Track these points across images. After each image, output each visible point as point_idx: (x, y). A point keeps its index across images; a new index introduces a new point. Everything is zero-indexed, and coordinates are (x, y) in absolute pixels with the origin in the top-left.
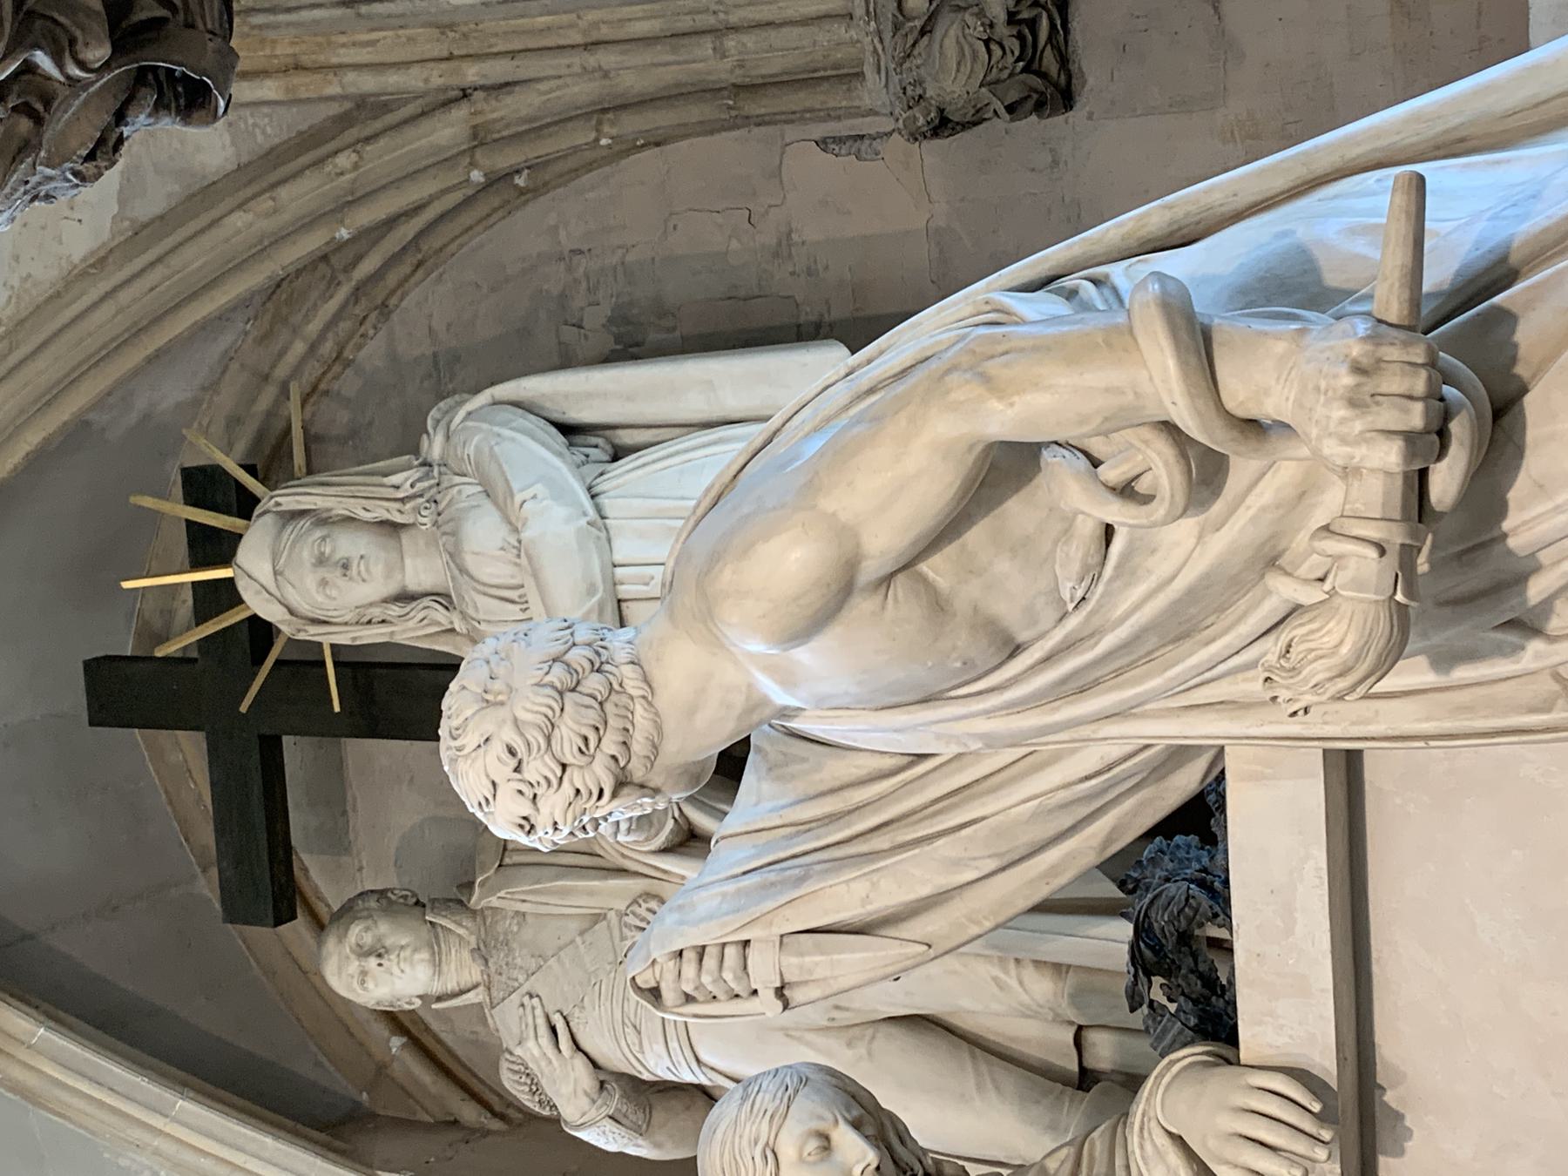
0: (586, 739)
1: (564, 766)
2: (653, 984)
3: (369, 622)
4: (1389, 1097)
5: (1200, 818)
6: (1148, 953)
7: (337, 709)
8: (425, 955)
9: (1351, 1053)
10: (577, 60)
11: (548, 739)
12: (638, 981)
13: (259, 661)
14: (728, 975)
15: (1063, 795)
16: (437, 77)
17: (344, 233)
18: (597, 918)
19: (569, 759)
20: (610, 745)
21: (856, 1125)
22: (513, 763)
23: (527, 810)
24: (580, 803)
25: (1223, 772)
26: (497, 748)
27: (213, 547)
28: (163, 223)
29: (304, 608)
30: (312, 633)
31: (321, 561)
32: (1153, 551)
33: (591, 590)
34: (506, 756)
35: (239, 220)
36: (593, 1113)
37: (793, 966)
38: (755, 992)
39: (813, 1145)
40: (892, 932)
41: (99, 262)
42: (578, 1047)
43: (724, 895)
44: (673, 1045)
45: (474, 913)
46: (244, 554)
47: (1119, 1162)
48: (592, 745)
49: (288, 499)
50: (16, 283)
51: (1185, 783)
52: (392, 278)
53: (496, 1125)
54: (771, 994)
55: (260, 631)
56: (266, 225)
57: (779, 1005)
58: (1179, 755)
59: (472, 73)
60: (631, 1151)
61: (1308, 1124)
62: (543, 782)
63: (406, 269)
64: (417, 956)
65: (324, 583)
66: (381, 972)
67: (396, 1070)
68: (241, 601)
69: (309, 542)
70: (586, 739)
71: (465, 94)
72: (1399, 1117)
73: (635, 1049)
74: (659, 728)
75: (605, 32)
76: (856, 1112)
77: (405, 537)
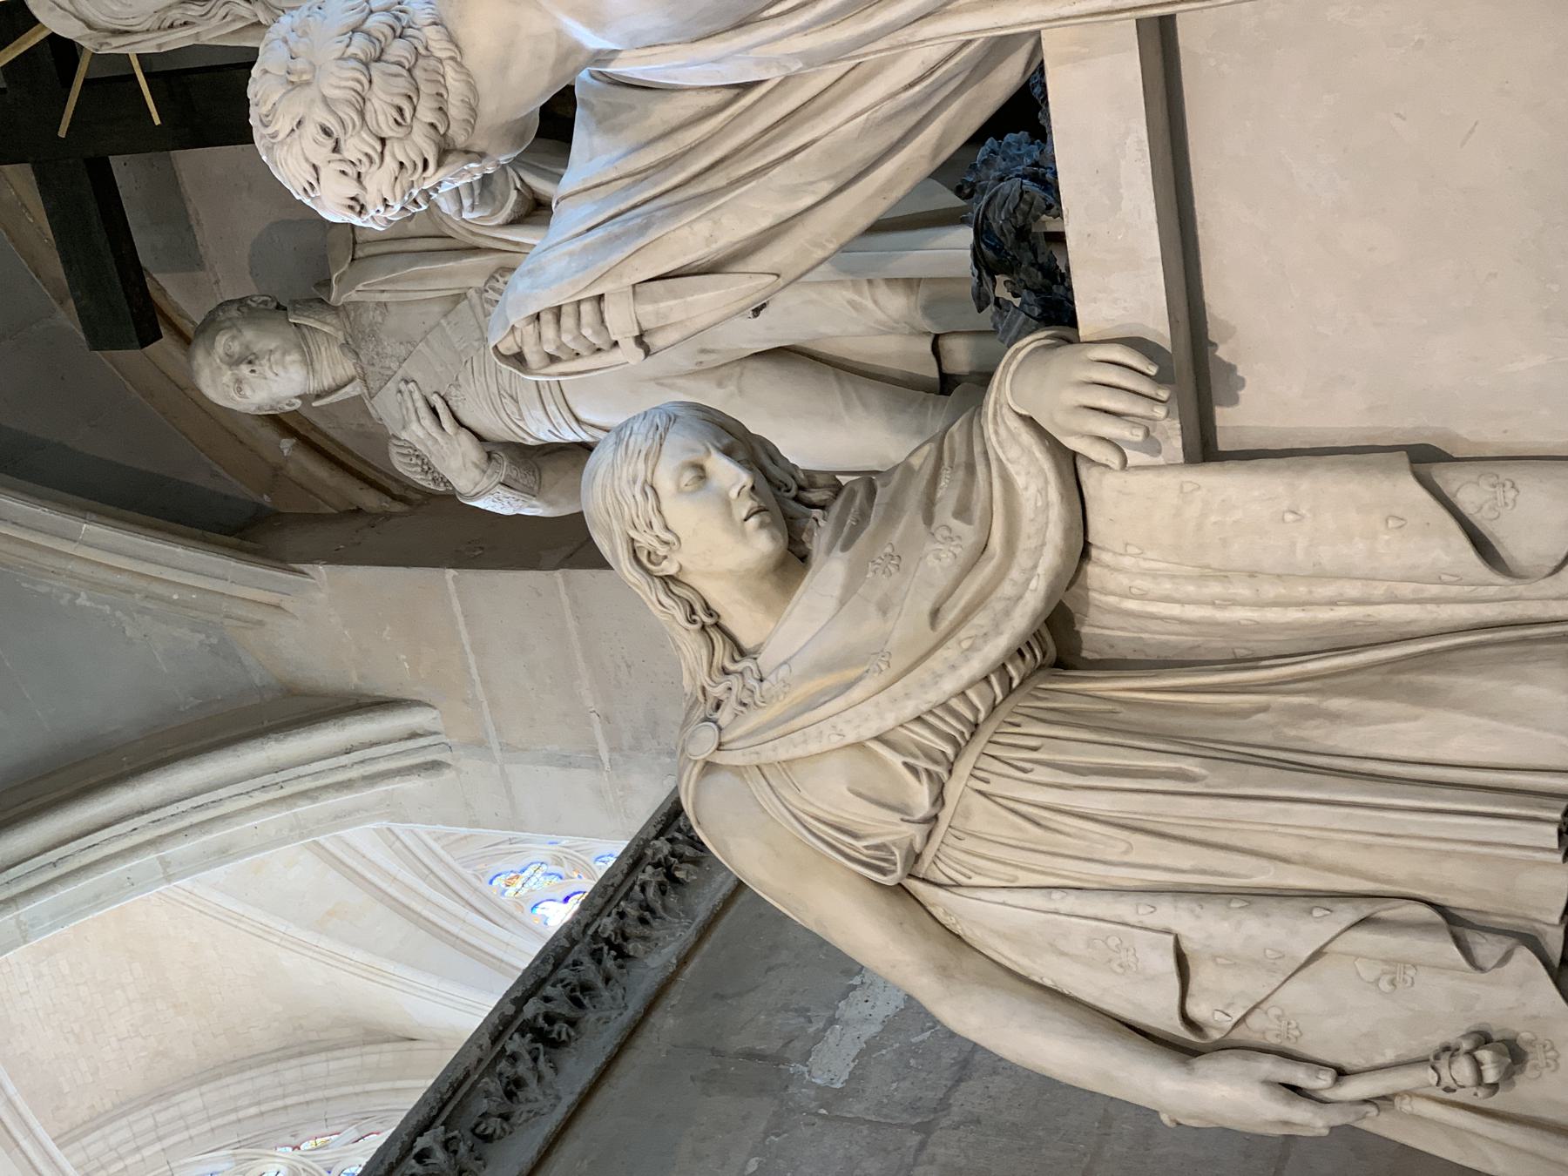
0: (400, 110)
1: (383, 141)
2: (516, 350)
3: (171, 26)
4: (1222, 352)
5: (1025, 112)
6: (989, 254)
7: (157, 121)
8: (295, 356)
9: (1182, 314)
11: (362, 114)
12: (501, 348)
13: (68, 84)
14: (587, 332)
15: (888, 108)
18: (458, 298)
19: (386, 133)
21: (728, 452)
22: (330, 143)
23: (353, 190)
24: (406, 177)
26: (311, 130)
29: (101, 19)
30: (115, 46)
34: (322, 137)
36: (485, 482)
37: (649, 313)
38: (616, 343)
39: (688, 476)
40: (740, 267)
43: (571, 254)
44: (552, 408)
45: (336, 309)
47: (977, 449)
48: (408, 114)
51: (1007, 77)
53: (398, 507)
54: (632, 343)
55: (63, 51)
57: (640, 352)
58: (1000, 47)
60: (527, 512)
61: (1145, 387)
62: (364, 159)
64: (288, 358)
66: (256, 377)
67: (292, 470)
68: (37, 22)
70: (400, 110)
72: (1231, 369)
73: (516, 417)
74: (472, 87)
76: (727, 440)
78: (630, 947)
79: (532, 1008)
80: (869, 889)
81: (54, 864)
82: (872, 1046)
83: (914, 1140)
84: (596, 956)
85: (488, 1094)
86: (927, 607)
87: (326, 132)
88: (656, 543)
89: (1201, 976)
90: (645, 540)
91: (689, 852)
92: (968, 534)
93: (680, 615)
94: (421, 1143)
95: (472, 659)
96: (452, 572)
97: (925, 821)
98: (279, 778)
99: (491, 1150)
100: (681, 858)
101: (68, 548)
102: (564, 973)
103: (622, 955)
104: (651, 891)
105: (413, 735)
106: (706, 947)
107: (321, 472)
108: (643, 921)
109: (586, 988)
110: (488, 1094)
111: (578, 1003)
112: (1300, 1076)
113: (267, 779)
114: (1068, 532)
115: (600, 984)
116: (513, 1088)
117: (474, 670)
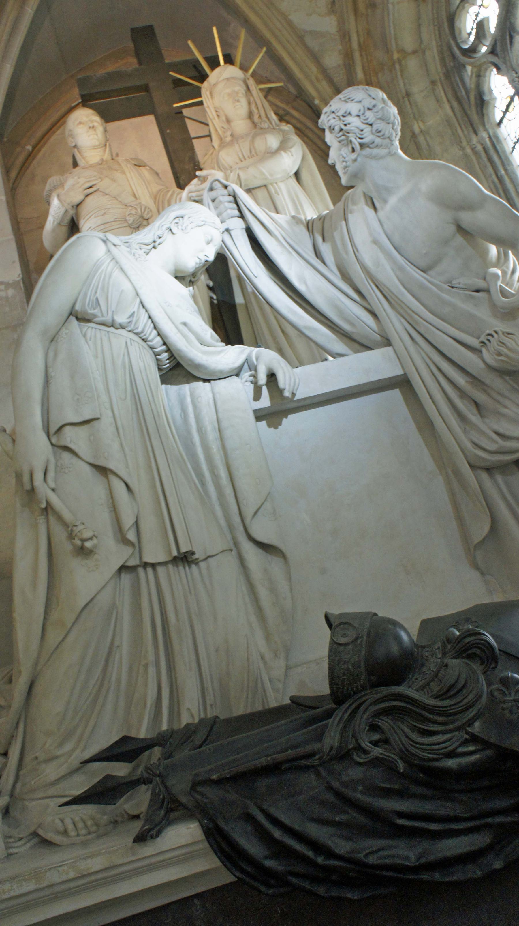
0: (379, 132)
1: (371, 125)
2: (215, 187)
3: (216, 111)
11: (380, 119)
18: (135, 197)
19: (375, 127)
20: (378, 141)
22: (370, 107)
24: (357, 131)
26: (374, 102)
28: (306, 46)
32: (475, 305)
33: (271, 175)
34: (373, 104)
36: (66, 205)
42: (87, 196)
46: (230, 67)
49: (251, 82)
54: (226, 227)
61: (291, 390)
62: (366, 118)
67: (18, 149)
69: (240, 89)
77: (248, 121)
86: (187, 321)
87: (374, 106)
89: (82, 432)
93: (159, 233)
97: (113, 321)
107: (21, 158)
112: (51, 474)
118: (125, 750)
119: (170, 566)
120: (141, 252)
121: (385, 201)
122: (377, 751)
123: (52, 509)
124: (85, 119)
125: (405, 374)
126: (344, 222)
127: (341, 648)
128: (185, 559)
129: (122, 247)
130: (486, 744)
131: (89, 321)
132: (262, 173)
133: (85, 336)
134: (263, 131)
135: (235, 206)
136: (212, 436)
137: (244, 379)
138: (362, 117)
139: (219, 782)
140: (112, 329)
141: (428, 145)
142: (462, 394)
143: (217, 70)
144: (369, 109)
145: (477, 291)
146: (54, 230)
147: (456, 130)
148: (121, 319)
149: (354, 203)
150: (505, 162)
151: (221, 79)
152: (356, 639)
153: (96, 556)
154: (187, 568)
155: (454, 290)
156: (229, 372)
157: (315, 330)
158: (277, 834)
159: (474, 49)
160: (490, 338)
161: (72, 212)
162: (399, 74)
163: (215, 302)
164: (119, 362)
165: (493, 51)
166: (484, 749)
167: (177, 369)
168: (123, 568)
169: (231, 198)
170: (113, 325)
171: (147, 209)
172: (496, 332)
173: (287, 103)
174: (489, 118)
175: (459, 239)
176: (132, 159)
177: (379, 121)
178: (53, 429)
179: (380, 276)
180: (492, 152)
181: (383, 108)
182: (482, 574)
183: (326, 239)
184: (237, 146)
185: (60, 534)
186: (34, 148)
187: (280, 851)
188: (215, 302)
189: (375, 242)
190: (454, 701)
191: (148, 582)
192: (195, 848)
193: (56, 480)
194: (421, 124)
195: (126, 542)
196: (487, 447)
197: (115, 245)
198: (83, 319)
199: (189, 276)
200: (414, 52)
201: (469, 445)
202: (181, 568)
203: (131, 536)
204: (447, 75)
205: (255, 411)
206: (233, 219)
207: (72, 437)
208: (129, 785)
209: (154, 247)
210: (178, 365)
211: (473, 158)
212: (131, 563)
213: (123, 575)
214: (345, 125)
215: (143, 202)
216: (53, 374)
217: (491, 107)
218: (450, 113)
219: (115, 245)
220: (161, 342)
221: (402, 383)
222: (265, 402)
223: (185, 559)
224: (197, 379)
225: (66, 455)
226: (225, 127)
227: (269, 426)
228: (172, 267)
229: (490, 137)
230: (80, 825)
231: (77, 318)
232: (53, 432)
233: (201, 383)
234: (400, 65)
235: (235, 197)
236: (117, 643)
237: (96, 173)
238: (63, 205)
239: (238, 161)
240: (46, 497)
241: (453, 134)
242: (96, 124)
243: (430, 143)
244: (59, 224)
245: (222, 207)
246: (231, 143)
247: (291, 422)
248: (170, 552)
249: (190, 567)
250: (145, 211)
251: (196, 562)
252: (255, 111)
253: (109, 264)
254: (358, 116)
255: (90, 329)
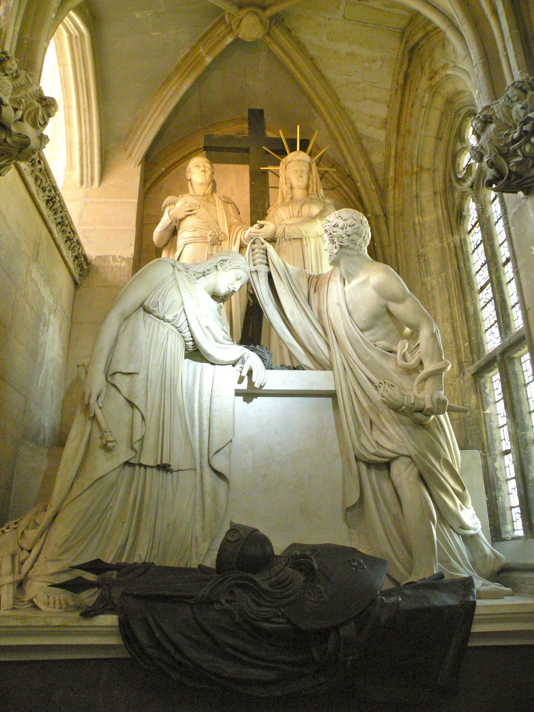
1: (349, 236)
7: (261, 168)
8: (204, 181)
10: (392, 240)
11: (356, 233)
14: (260, 260)
16: (390, 210)
17: (359, 184)
18: (218, 224)
20: (351, 246)
22: (351, 225)
23: (340, 226)
25: (304, 369)
26: (354, 222)
27: (304, 147)
31: (302, 171)
32: (387, 360)
33: (306, 233)
35: (363, 162)
39: (239, 277)
41: (355, 129)
44: (191, 239)
45: (212, 193)
46: (302, 153)
49: (314, 165)
50: (353, 110)
52: (341, 192)
55: (283, 154)
56: (361, 168)
59: (391, 218)
61: (260, 383)
63: (344, 195)
65: (296, 171)
66: (197, 170)
67: (156, 169)
69: (306, 168)
71: (385, 215)
75: (398, 247)
77: (305, 191)
78: (60, 226)
79: (57, 197)
80: (143, 299)
81: (81, 81)
82: (37, 284)
83: (23, 293)
84: (62, 217)
85: (46, 182)
87: (354, 225)
88: (226, 266)
89: (127, 378)
90: (227, 264)
91: (72, 246)
92: (220, 338)
93: (209, 268)
94: (42, 162)
95: (112, 200)
96: (136, 201)
97: (164, 317)
98: (88, 143)
99: (34, 179)
100: (72, 244)
101: (158, 112)
102: (60, 209)
103: (60, 223)
104: (68, 234)
105: (92, 180)
106: (54, 246)
107: (157, 175)
108: (63, 231)
109: (55, 213)
110: (46, 182)
111: (54, 210)
112: (101, 399)
113: (88, 140)
114: (222, 361)
115: (55, 217)
116: (44, 190)
117: (108, 200)
118: (96, 566)
119: (155, 470)
120: (193, 277)
121: (349, 282)
122: (226, 605)
123: (97, 419)
124: (201, 164)
125: (335, 391)
126: (326, 285)
127: (228, 543)
128: (164, 468)
129: (184, 272)
130: (289, 621)
131: (150, 313)
132: (301, 231)
133: (145, 322)
134: (312, 202)
135: (265, 257)
136: (206, 398)
137: (236, 369)
138: (344, 230)
139: (136, 597)
140: (162, 321)
141: (421, 233)
142: (364, 413)
143: (293, 153)
144: (350, 226)
145: (391, 352)
146: (161, 232)
147: (442, 229)
148: (169, 317)
149: (335, 277)
150: (466, 259)
151: (296, 159)
152: (238, 540)
153: (112, 452)
154: (165, 473)
155: (377, 348)
156: (227, 362)
157: (294, 347)
158: (158, 634)
159: (463, 180)
160: (381, 385)
161: (174, 224)
162: (415, 181)
163: (251, 305)
164: (160, 343)
165: (472, 187)
166: (287, 623)
167: (196, 353)
168: (127, 463)
169: (264, 252)
170: (163, 319)
171: (222, 235)
172: (385, 382)
173: (341, 179)
174: (463, 227)
175: (387, 318)
176: (224, 197)
177: (354, 235)
178: (110, 373)
179: (337, 328)
180: (459, 250)
181: (359, 227)
182: (349, 527)
183: (316, 291)
184: (291, 207)
185: (97, 434)
186: (166, 170)
187: (158, 645)
188: (251, 305)
189: (339, 304)
190: (279, 591)
191: (139, 475)
192: (112, 629)
193: (103, 402)
194: (420, 218)
195: (133, 449)
196: (369, 450)
197: (179, 270)
198: (147, 311)
199: (223, 296)
200: (428, 170)
201: (357, 445)
202: (161, 472)
203: (136, 446)
204: (445, 190)
205: (236, 390)
206: (262, 265)
207: (119, 380)
208: (90, 585)
209: (204, 275)
210: (198, 350)
211: (448, 250)
212: (131, 461)
213: (126, 467)
214: (334, 232)
215: (222, 229)
216: (120, 340)
217: (466, 221)
218: (441, 217)
219: (179, 270)
220: (190, 335)
221: (332, 395)
222: (244, 386)
223: (164, 468)
224: (207, 362)
225: (113, 390)
226: (289, 192)
227: (244, 400)
228: (211, 289)
229: (460, 240)
230: (57, 602)
231: (144, 310)
232: (110, 375)
233: (209, 364)
234: (417, 174)
235: (266, 251)
236: (111, 505)
237: (197, 202)
238: (170, 218)
239: (288, 217)
240: (95, 410)
241: (439, 230)
242: (207, 169)
243: (423, 233)
244: (166, 229)
245: (257, 256)
246: (287, 205)
247: (258, 401)
248: (157, 461)
249: (167, 473)
250: (221, 235)
251: (171, 471)
252: (311, 185)
253: (171, 281)
254: (343, 229)
255: (149, 319)
